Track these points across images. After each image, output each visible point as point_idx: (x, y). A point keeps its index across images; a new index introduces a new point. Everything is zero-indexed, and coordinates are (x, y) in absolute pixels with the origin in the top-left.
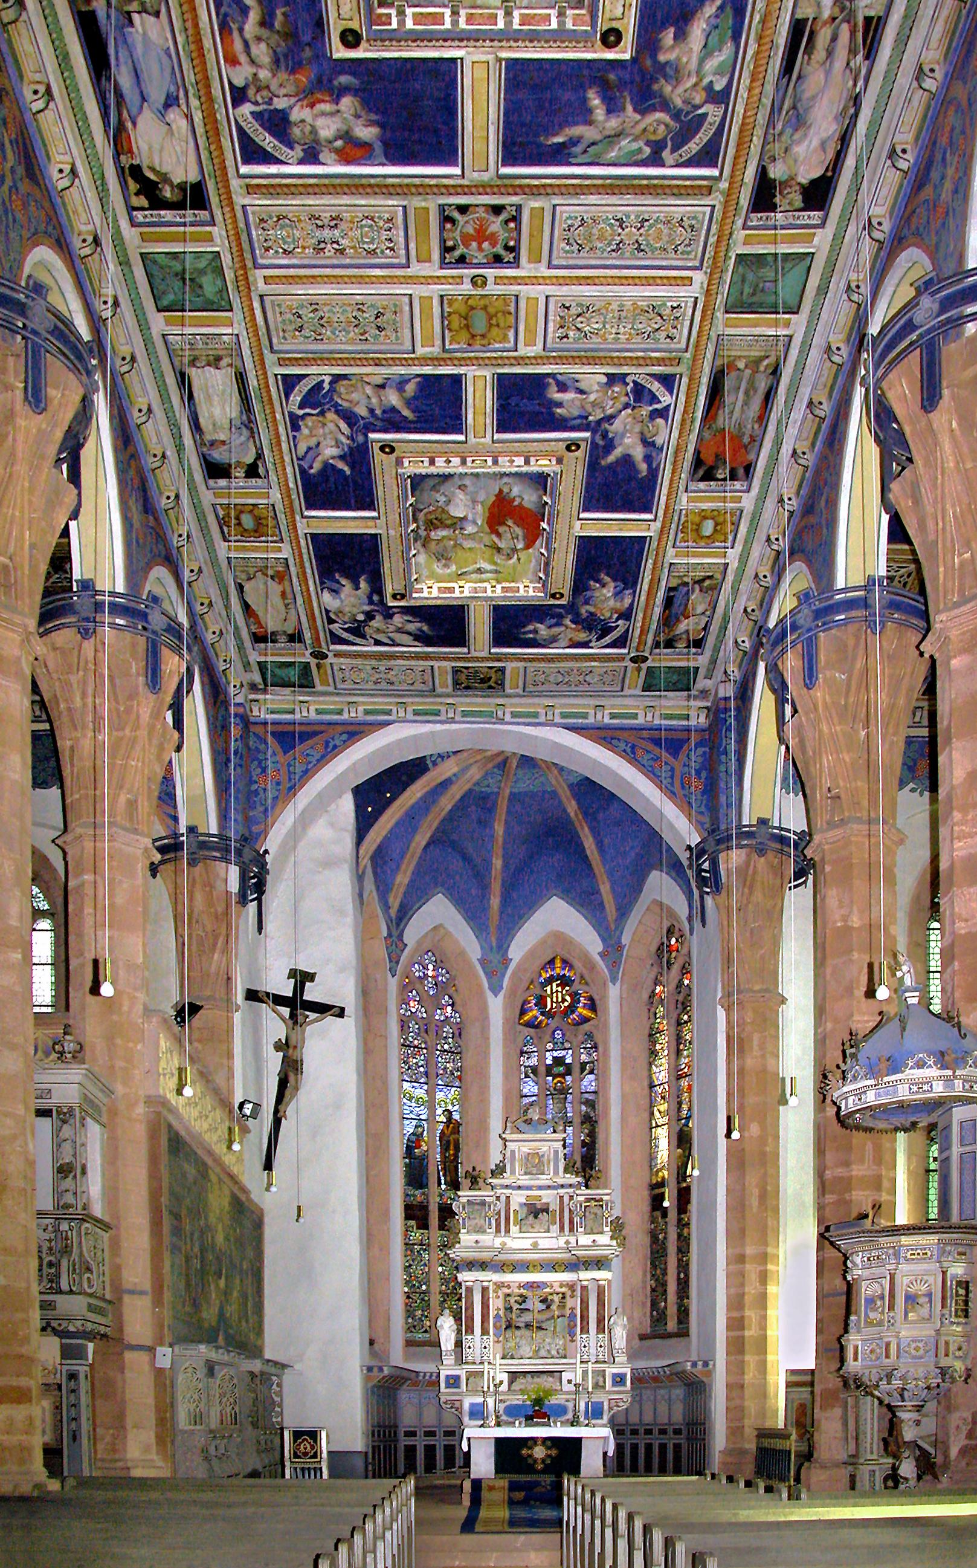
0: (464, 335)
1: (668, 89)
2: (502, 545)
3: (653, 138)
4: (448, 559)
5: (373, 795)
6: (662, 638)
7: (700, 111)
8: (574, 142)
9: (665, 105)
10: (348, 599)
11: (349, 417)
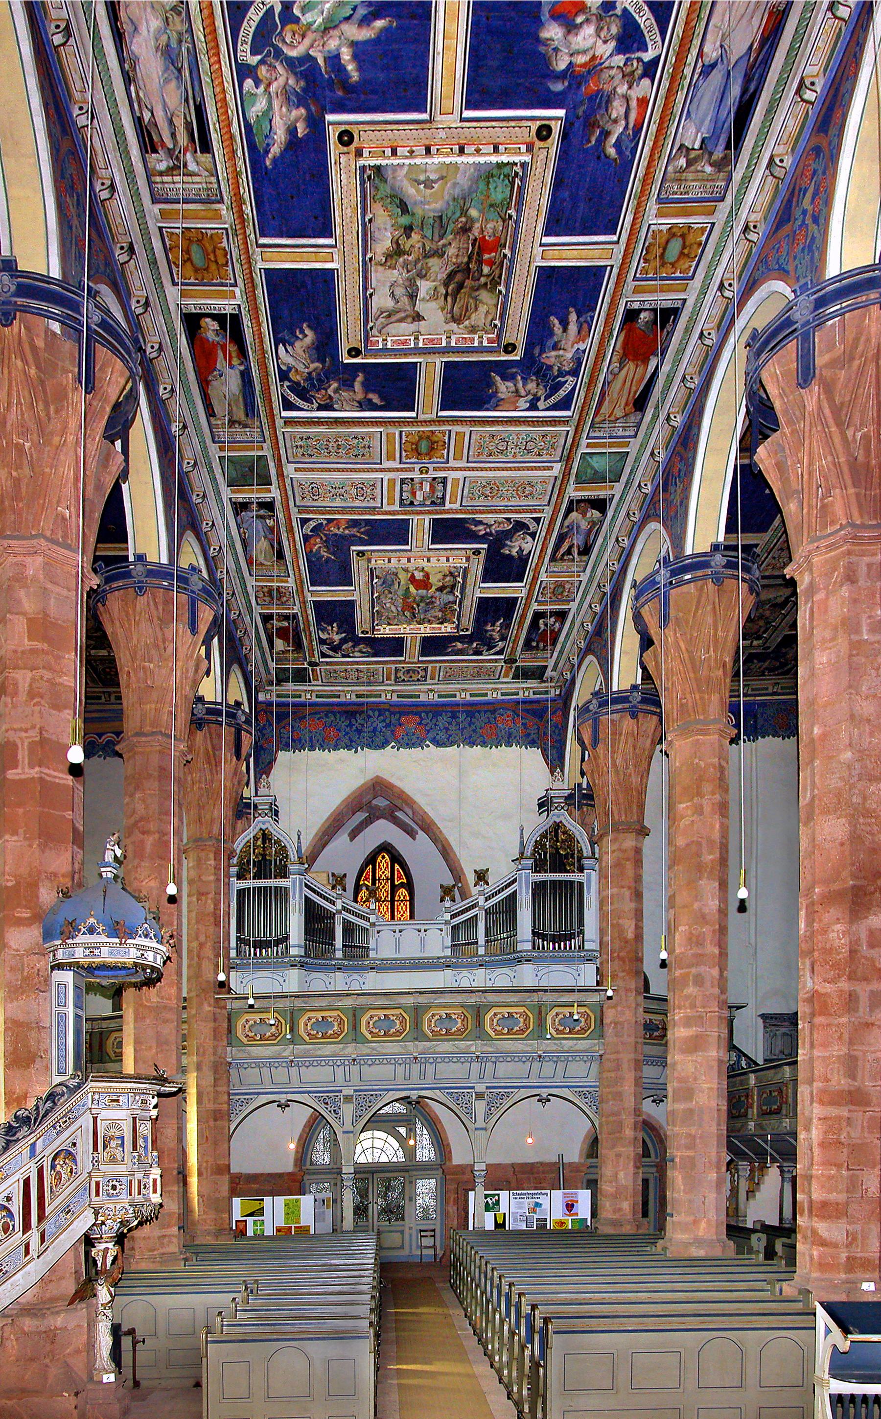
1: (291, 82)
3: (295, 27)
7: (259, 57)
9: (291, 64)
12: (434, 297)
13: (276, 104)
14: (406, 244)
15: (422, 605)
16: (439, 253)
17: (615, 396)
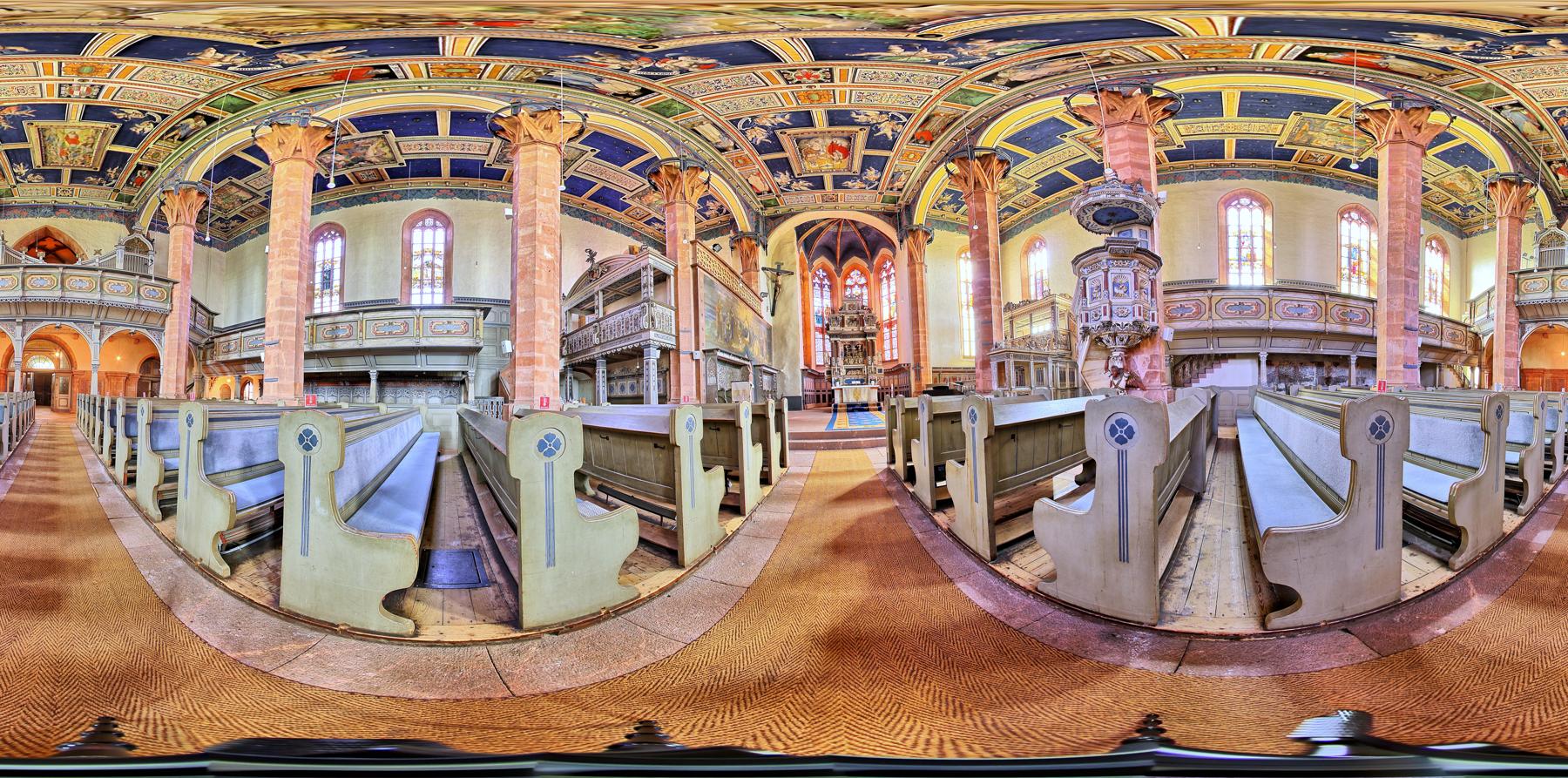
5: (800, 230)
10: (784, 178)
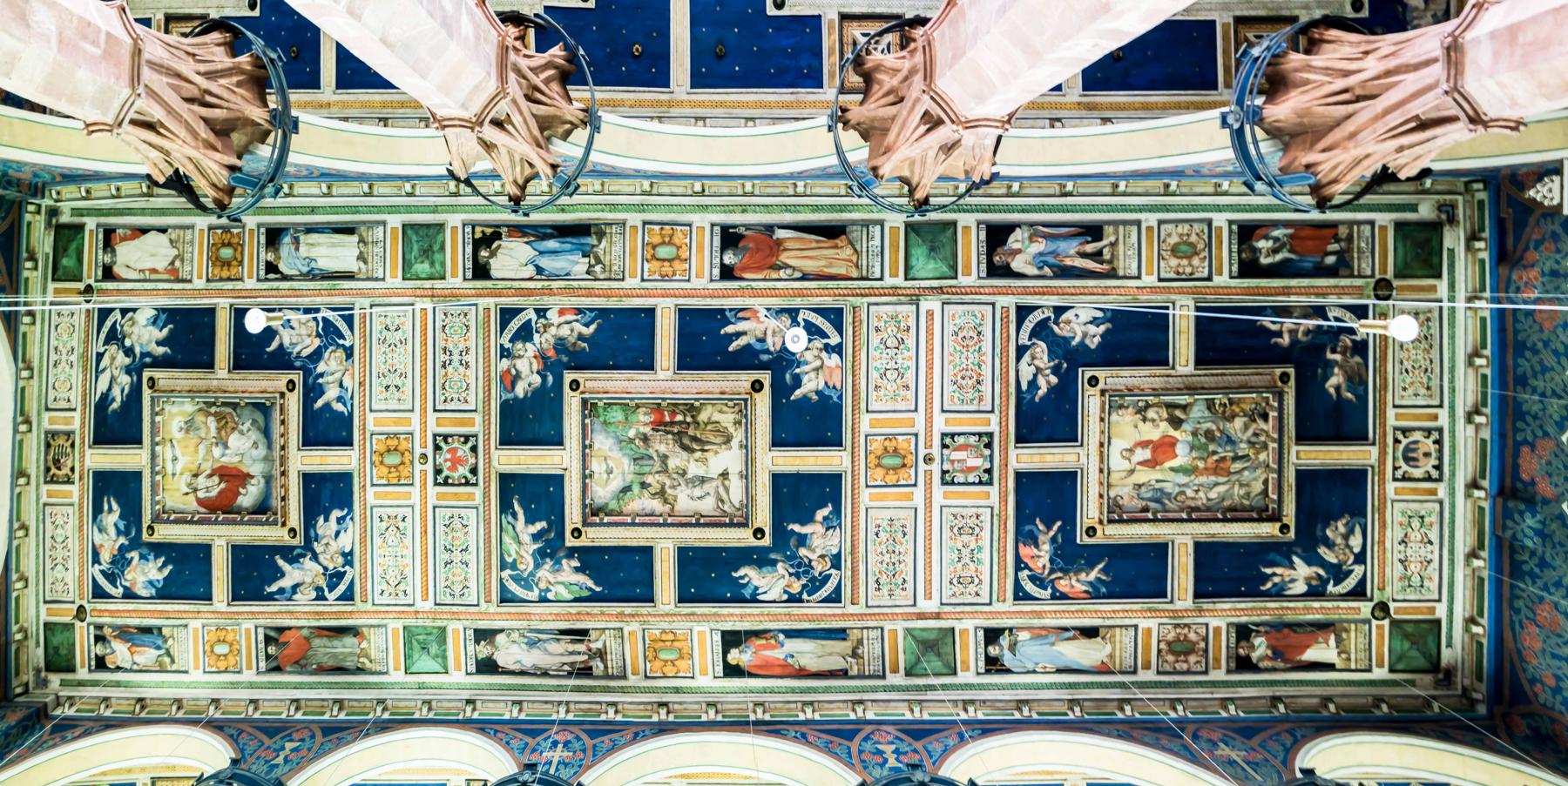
0: (382, 448)
1: (547, 567)
2: (201, 479)
4: (187, 431)
6: (107, 631)
8: (515, 515)
9: (537, 566)
11: (317, 355)
12: (704, 461)
13: (560, 579)
14: (655, 488)
15: (1212, 447)
16: (664, 458)
17: (823, 263)
